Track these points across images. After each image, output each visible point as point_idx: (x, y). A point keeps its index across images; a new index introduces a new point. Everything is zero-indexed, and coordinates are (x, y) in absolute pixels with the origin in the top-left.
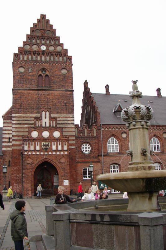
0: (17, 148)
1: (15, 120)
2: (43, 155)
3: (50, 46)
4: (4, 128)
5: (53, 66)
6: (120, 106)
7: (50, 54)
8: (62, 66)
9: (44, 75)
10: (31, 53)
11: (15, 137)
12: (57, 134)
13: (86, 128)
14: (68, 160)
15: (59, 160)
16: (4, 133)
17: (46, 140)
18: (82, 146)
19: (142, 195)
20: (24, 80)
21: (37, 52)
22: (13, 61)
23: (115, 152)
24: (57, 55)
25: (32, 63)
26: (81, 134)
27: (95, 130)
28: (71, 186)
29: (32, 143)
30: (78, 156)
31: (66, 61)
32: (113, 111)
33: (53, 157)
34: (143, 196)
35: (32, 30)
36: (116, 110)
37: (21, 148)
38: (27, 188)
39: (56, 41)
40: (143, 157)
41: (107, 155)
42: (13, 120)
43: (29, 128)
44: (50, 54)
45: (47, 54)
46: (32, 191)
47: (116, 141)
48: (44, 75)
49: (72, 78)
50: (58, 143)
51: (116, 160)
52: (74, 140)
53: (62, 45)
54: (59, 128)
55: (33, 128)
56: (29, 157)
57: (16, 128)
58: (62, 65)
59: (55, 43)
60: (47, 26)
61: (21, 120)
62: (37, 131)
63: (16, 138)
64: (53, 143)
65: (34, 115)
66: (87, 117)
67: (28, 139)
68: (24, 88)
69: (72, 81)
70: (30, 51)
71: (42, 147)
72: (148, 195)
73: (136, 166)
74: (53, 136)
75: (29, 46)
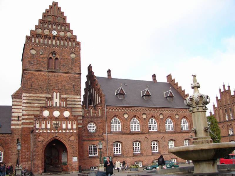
0: (27, 126)
2: (54, 133)
3: (61, 31)
4: (13, 107)
5: (63, 50)
6: (122, 89)
7: (60, 38)
8: (71, 50)
10: (42, 37)
12: (67, 114)
13: (91, 108)
14: (77, 138)
15: (69, 138)
17: (56, 119)
18: (88, 126)
19: (208, 163)
20: (35, 62)
21: (48, 37)
22: (25, 43)
23: (118, 131)
24: (67, 40)
25: (44, 46)
26: (87, 114)
27: (100, 110)
28: (79, 162)
29: (43, 122)
30: (84, 134)
31: (75, 46)
32: (116, 94)
33: (63, 135)
34: (209, 163)
35: (44, 15)
36: (118, 93)
37: (32, 126)
38: (38, 165)
39: (66, 27)
40: (205, 133)
41: (111, 133)
42: (23, 99)
43: (41, 107)
44: (60, 38)
45: (57, 39)
46: (43, 168)
47: (118, 121)
48: (54, 58)
49: (80, 62)
50: (68, 122)
51: (118, 138)
52: (80, 120)
53: (71, 31)
54: (69, 108)
55: (45, 107)
56: (40, 135)
57: (27, 107)
58: (71, 49)
59: (66, 29)
60: (59, 13)
61: (31, 100)
62: (49, 111)
63: (26, 117)
64: (63, 122)
65: (44, 95)
66: (90, 98)
67: (39, 118)
68: (35, 70)
69: (80, 65)
70: (42, 35)
71: (53, 125)
72: (212, 162)
73: (201, 140)
74: (63, 115)
75: (41, 30)
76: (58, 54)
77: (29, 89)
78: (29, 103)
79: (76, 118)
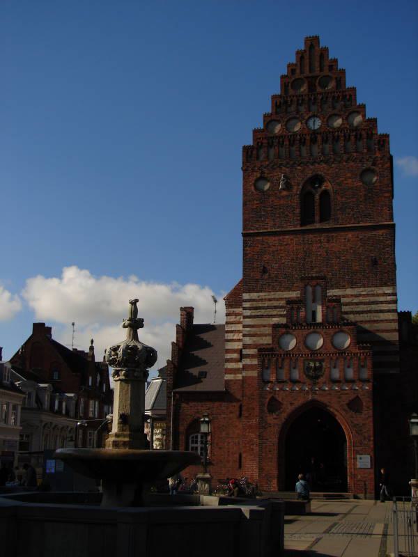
1: (250, 309)
10: (283, 142)
11: (250, 348)
16: (229, 338)
17: (314, 353)
24: (349, 136)
43: (275, 326)
45: (323, 139)
68: (269, 230)
70: (282, 137)
77: (257, 281)
79: (367, 351)
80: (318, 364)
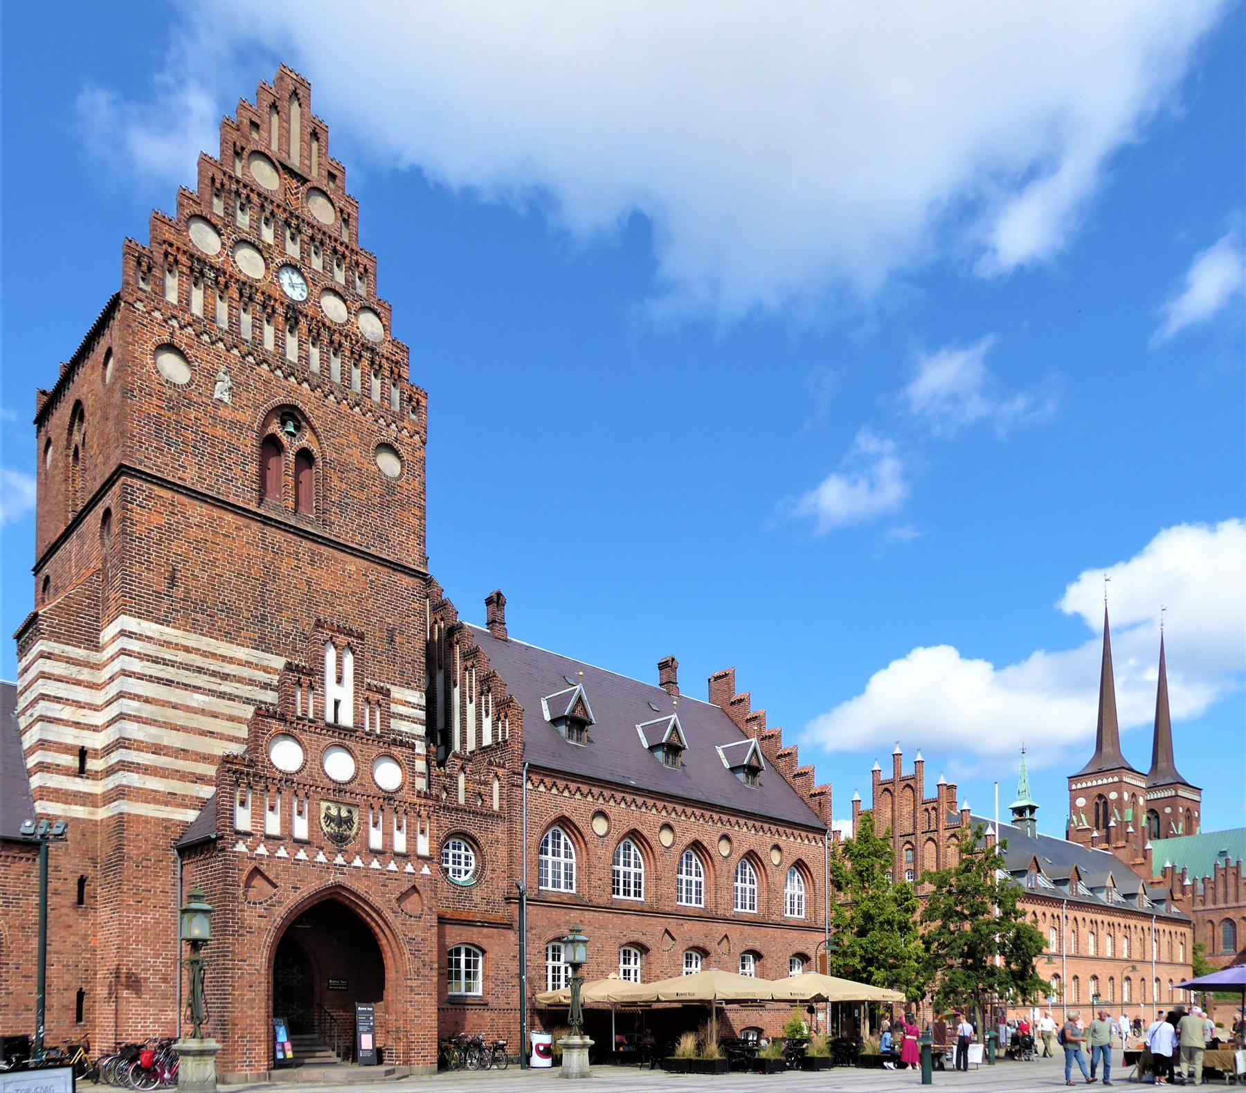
9: (292, 447)
17: (339, 790)
76: (313, 429)
78: (159, 680)
80: (344, 814)
